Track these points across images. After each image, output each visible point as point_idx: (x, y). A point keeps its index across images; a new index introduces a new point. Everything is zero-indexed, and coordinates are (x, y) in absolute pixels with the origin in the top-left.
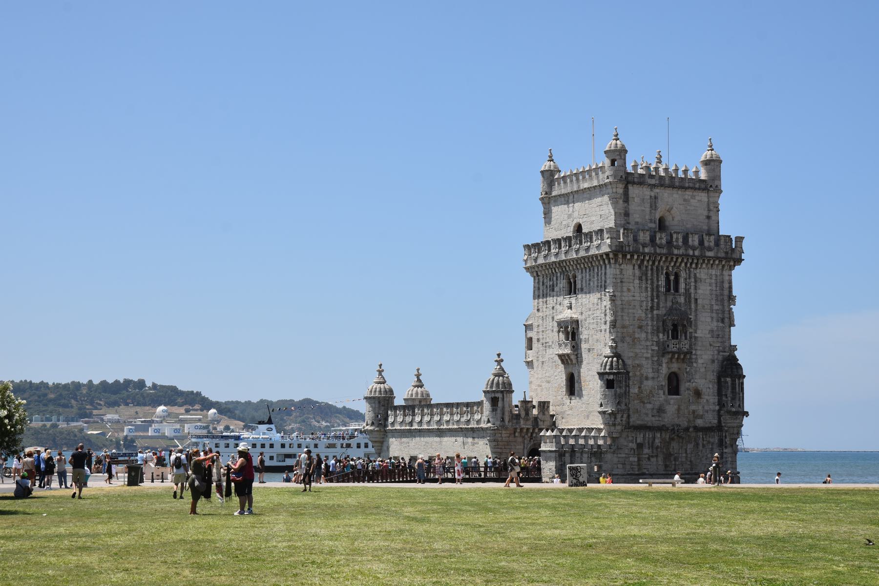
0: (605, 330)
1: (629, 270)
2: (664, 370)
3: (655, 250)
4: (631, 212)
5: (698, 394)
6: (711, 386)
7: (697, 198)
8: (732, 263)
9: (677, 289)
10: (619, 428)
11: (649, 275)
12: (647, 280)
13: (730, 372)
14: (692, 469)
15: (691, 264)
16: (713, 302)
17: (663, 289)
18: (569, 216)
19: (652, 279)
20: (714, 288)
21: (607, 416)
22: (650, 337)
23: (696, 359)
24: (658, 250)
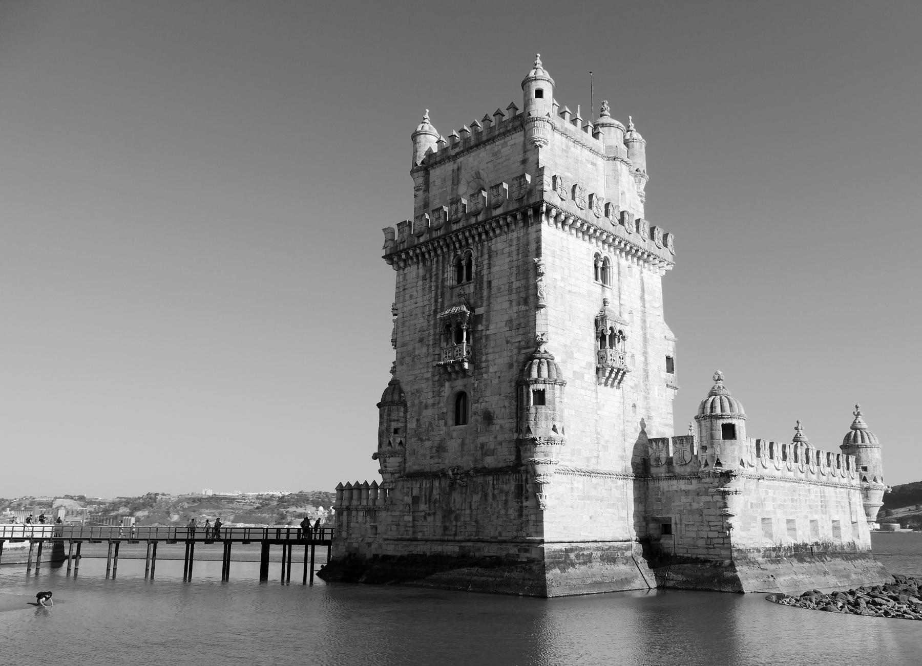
2: (447, 390)
3: (431, 235)
4: (431, 200)
5: (488, 418)
6: (507, 404)
7: (509, 143)
9: (469, 278)
12: (431, 278)
14: (477, 533)
15: (480, 235)
16: (513, 279)
20: (515, 258)
22: (431, 350)
23: (488, 367)
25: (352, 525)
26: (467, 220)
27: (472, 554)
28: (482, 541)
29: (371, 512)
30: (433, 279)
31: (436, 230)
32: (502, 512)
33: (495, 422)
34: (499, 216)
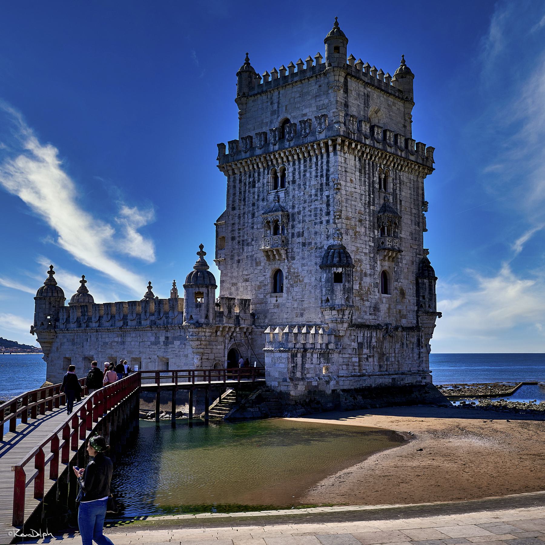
0: (328, 222)
1: (352, 161)
3: (374, 143)
4: (350, 104)
5: (402, 293)
6: (411, 287)
7: (396, 105)
8: (426, 171)
10: (346, 325)
11: (367, 169)
13: (425, 274)
17: (377, 186)
18: (273, 113)
19: (369, 174)
21: (334, 312)
22: (368, 232)
23: (401, 259)
24: (376, 145)
25: (307, 366)
26: (396, 150)
27: (399, 383)
28: (403, 374)
29: (325, 354)
30: (367, 176)
31: (377, 142)
32: (411, 355)
33: (406, 297)
34: (415, 162)
